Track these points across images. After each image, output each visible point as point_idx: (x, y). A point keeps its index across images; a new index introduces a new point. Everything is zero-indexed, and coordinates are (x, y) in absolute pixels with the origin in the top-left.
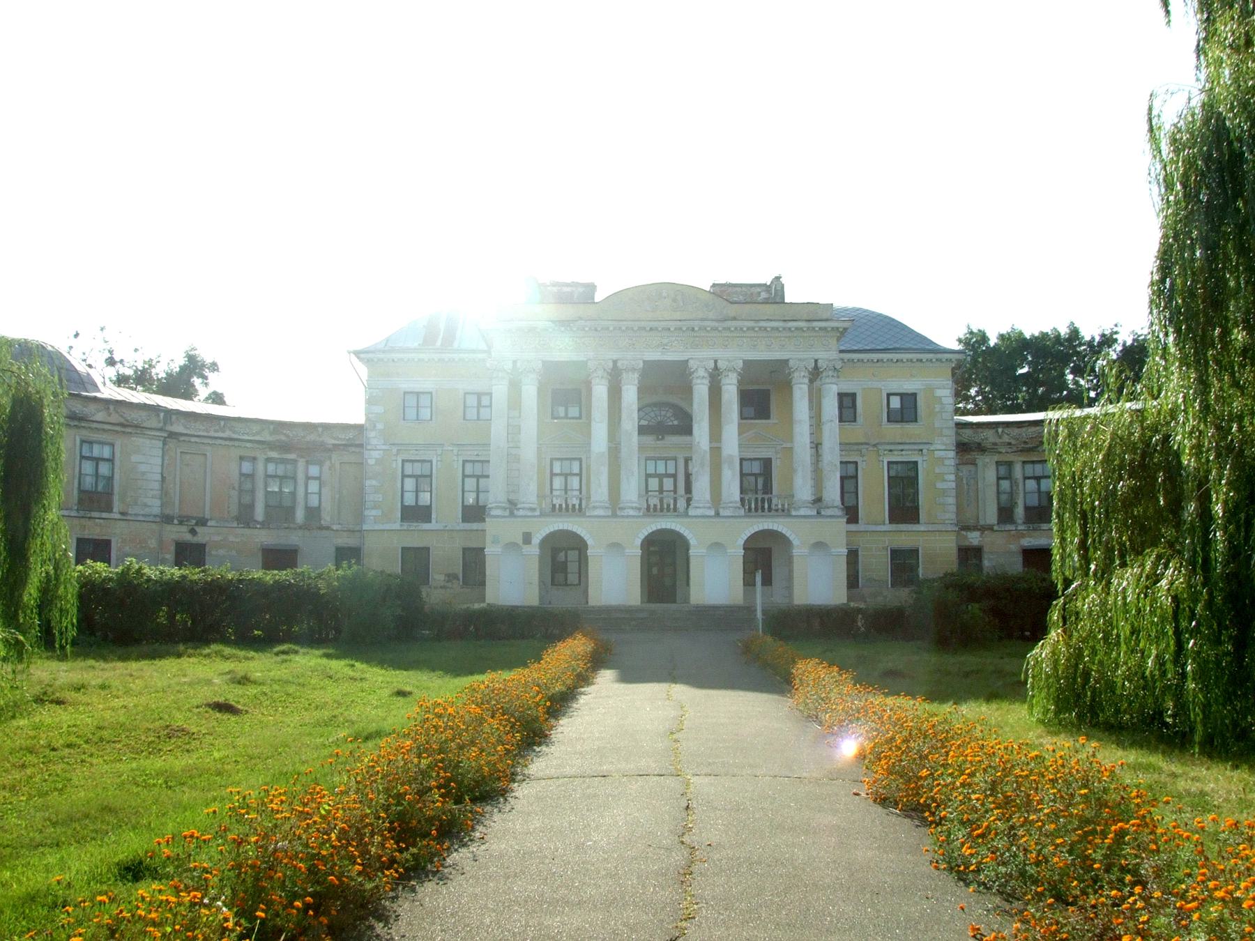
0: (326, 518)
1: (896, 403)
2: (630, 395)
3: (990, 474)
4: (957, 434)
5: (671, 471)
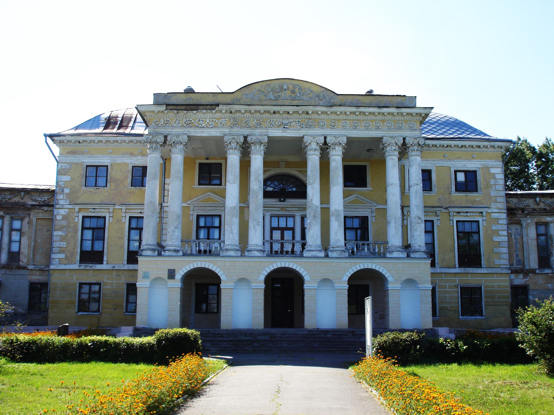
0: (24, 260)
1: (461, 177)
2: (257, 161)
3: (532, 232)
4: (507, 202)
5: (290, 225)
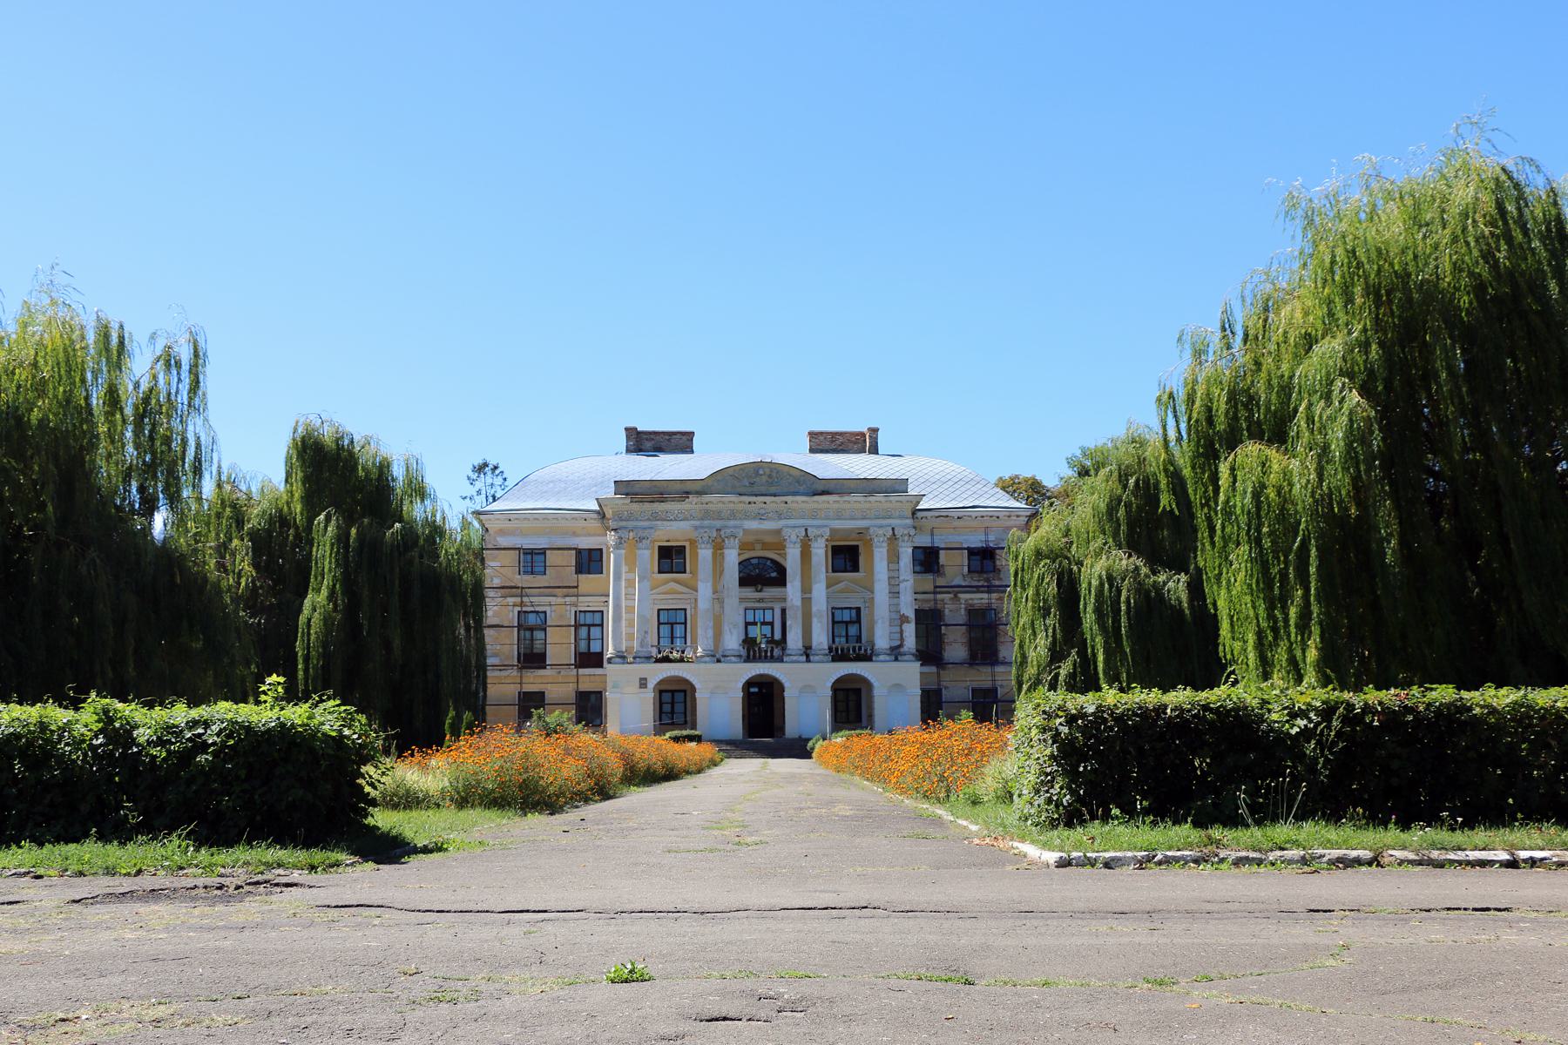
5: (768, 619)
